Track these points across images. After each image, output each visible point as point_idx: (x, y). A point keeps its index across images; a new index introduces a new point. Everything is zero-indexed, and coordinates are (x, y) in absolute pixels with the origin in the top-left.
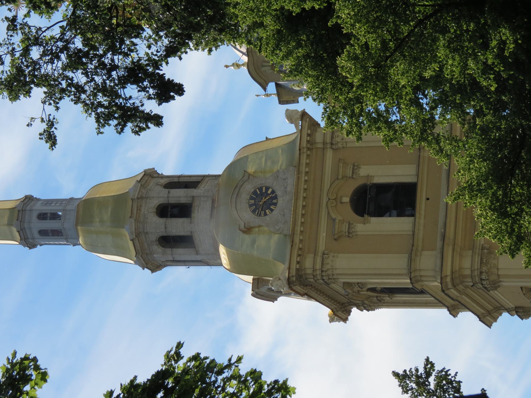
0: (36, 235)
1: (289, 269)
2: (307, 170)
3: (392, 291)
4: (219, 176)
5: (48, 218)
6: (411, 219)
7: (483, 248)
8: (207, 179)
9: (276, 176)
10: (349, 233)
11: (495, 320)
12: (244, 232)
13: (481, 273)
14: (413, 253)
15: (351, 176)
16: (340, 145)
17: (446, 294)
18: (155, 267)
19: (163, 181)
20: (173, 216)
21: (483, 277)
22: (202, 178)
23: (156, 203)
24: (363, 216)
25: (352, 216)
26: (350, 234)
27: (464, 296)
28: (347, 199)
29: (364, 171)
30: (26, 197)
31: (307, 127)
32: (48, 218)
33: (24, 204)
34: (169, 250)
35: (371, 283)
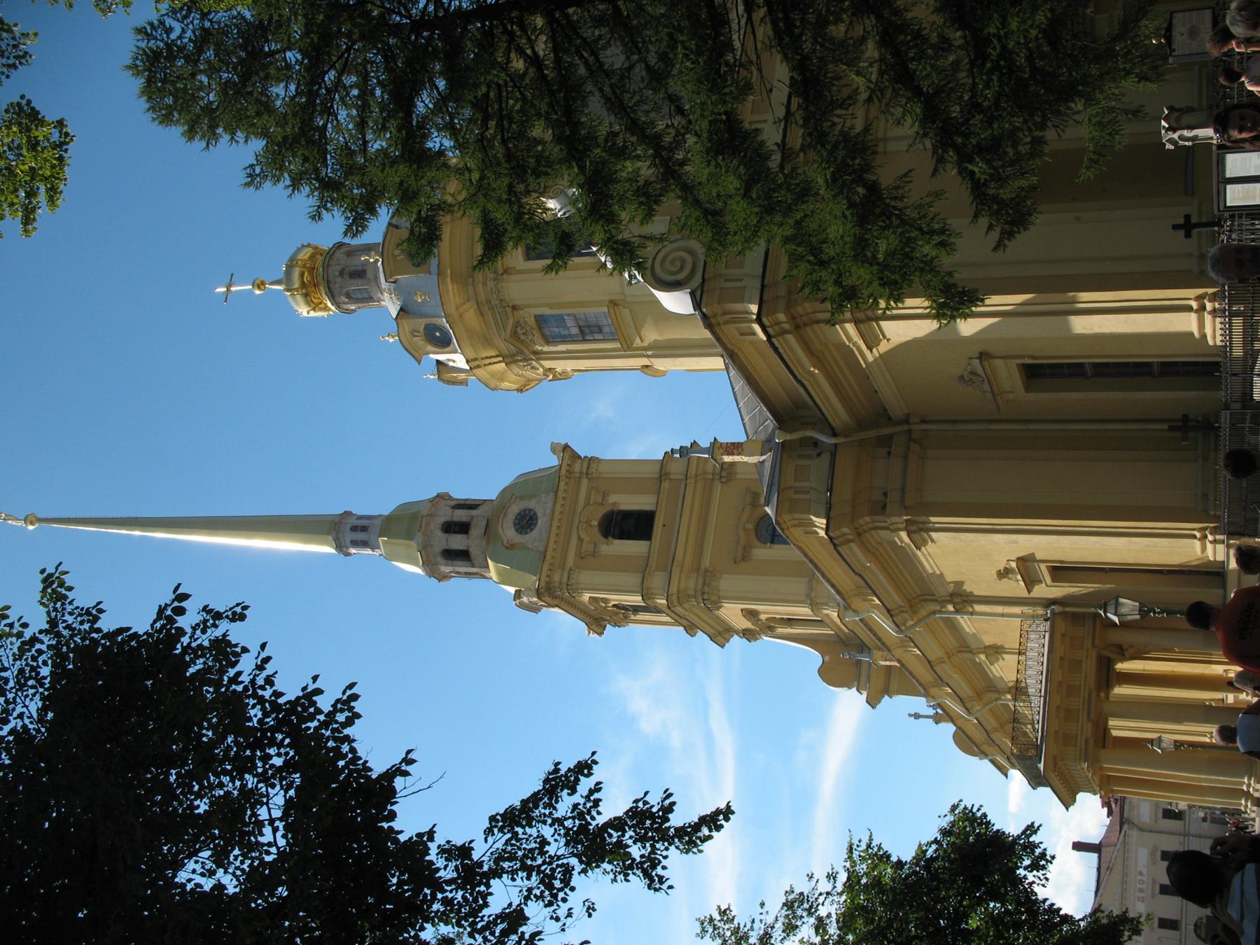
0: (348, 543)
2: (564, 495)
3: (636, 609)
6: (647, 543)
7: (706, 571)
8: (488, 502)
11: (728, 640)
12: (507, 548)
13: (703, 593)
14: (647, 572)
16: (594, 476)
17: (673, 611)
18: (442, 578)
19: (452, 503)
20: (455, 532)
21: (705, 597)
23: (442, 520)
24: (607, 538)
25: (598, 536)
26: (594, 554)
28: (595, 523)
29: (613, 498)
34: (450, 562)
35: (614, 600)
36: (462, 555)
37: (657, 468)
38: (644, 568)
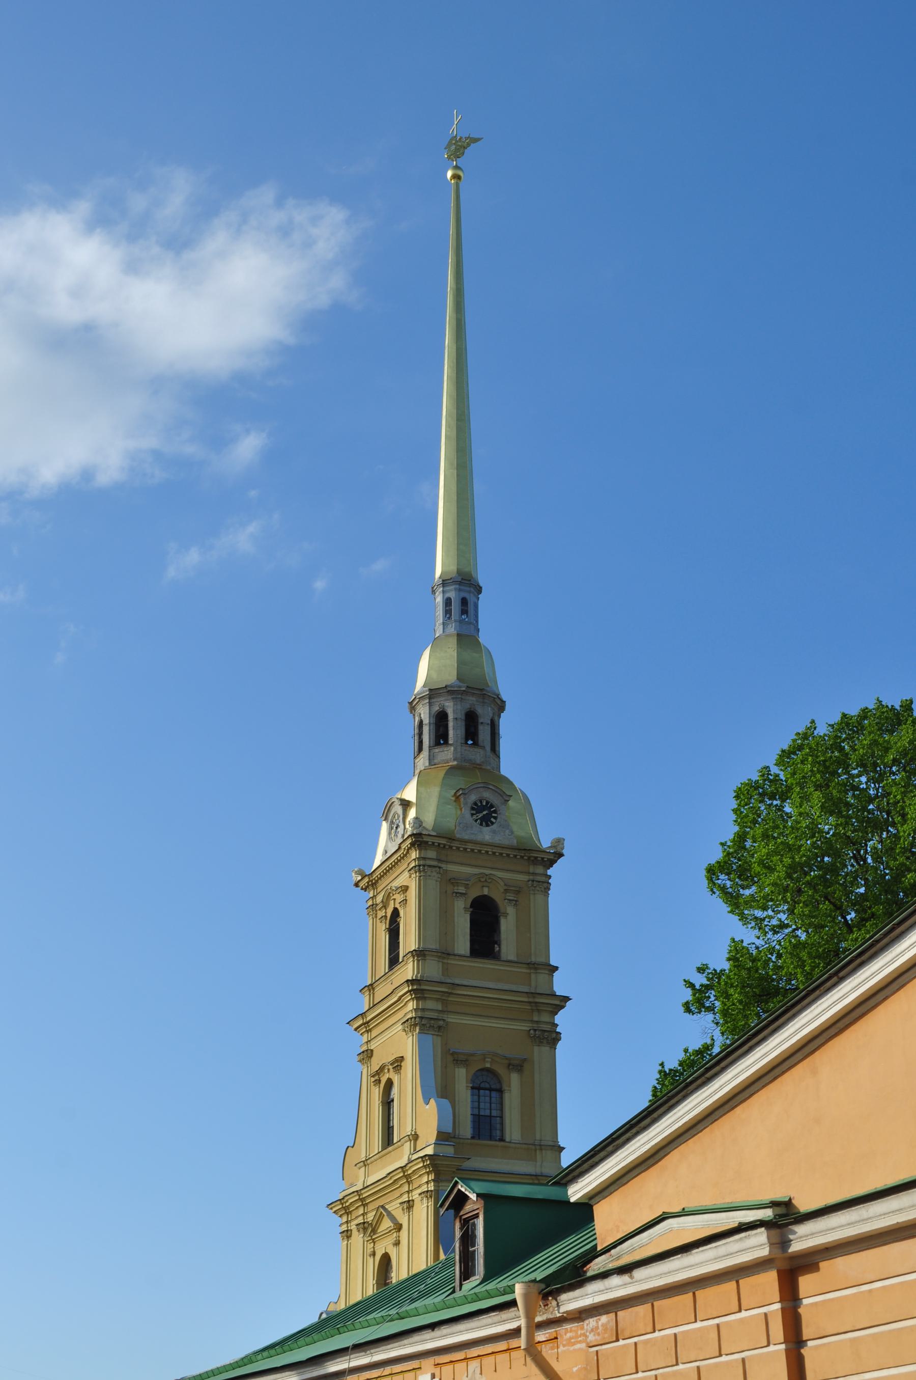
1: (429, 835)
4: (500, 772)
5: (463, 608)
6: (468, 952)
9: (506, 826)
10: (457, 893)
15: (507, 897)
19: (496, 718)
22: (498, 755)
23: (479, 710)
24: (471, 907)
27: (396, 999)
28: (486, 892)
30: (481, 588)
31: (549, 857)
32: (463, 608)
33: (476, 586)
34: (433, 720)
36: (441, 737)
37: (542, 959)
38: (445, 954)
